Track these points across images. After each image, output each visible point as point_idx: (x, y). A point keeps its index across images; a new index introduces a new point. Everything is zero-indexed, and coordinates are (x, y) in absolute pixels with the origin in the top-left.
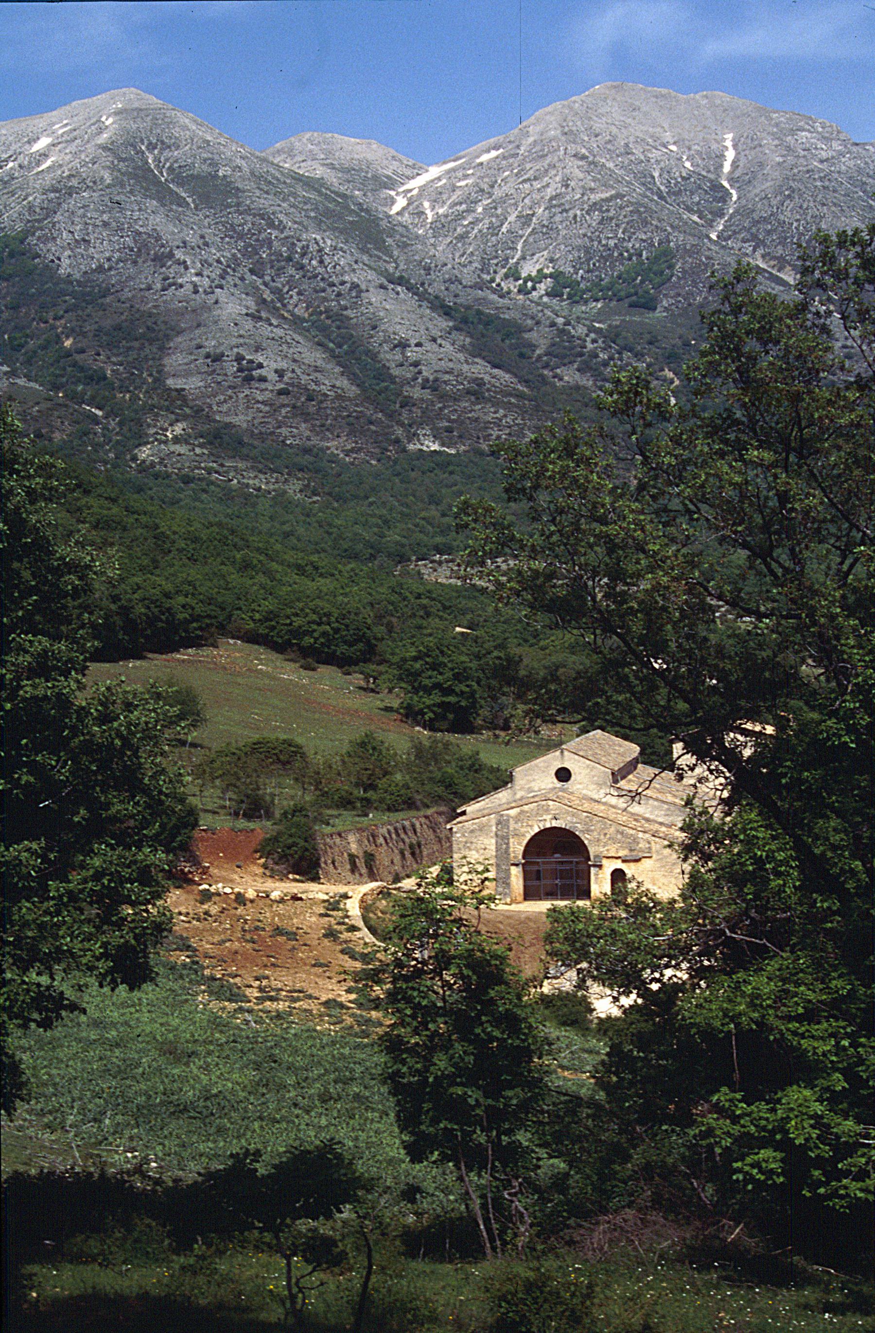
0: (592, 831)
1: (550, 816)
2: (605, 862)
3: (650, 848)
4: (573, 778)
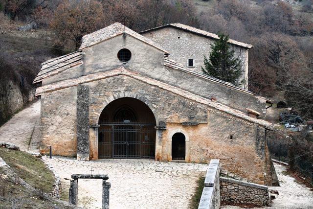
1: (123, 89)
2: (168, 128)
3: (206, 117)
4: (133, 57)
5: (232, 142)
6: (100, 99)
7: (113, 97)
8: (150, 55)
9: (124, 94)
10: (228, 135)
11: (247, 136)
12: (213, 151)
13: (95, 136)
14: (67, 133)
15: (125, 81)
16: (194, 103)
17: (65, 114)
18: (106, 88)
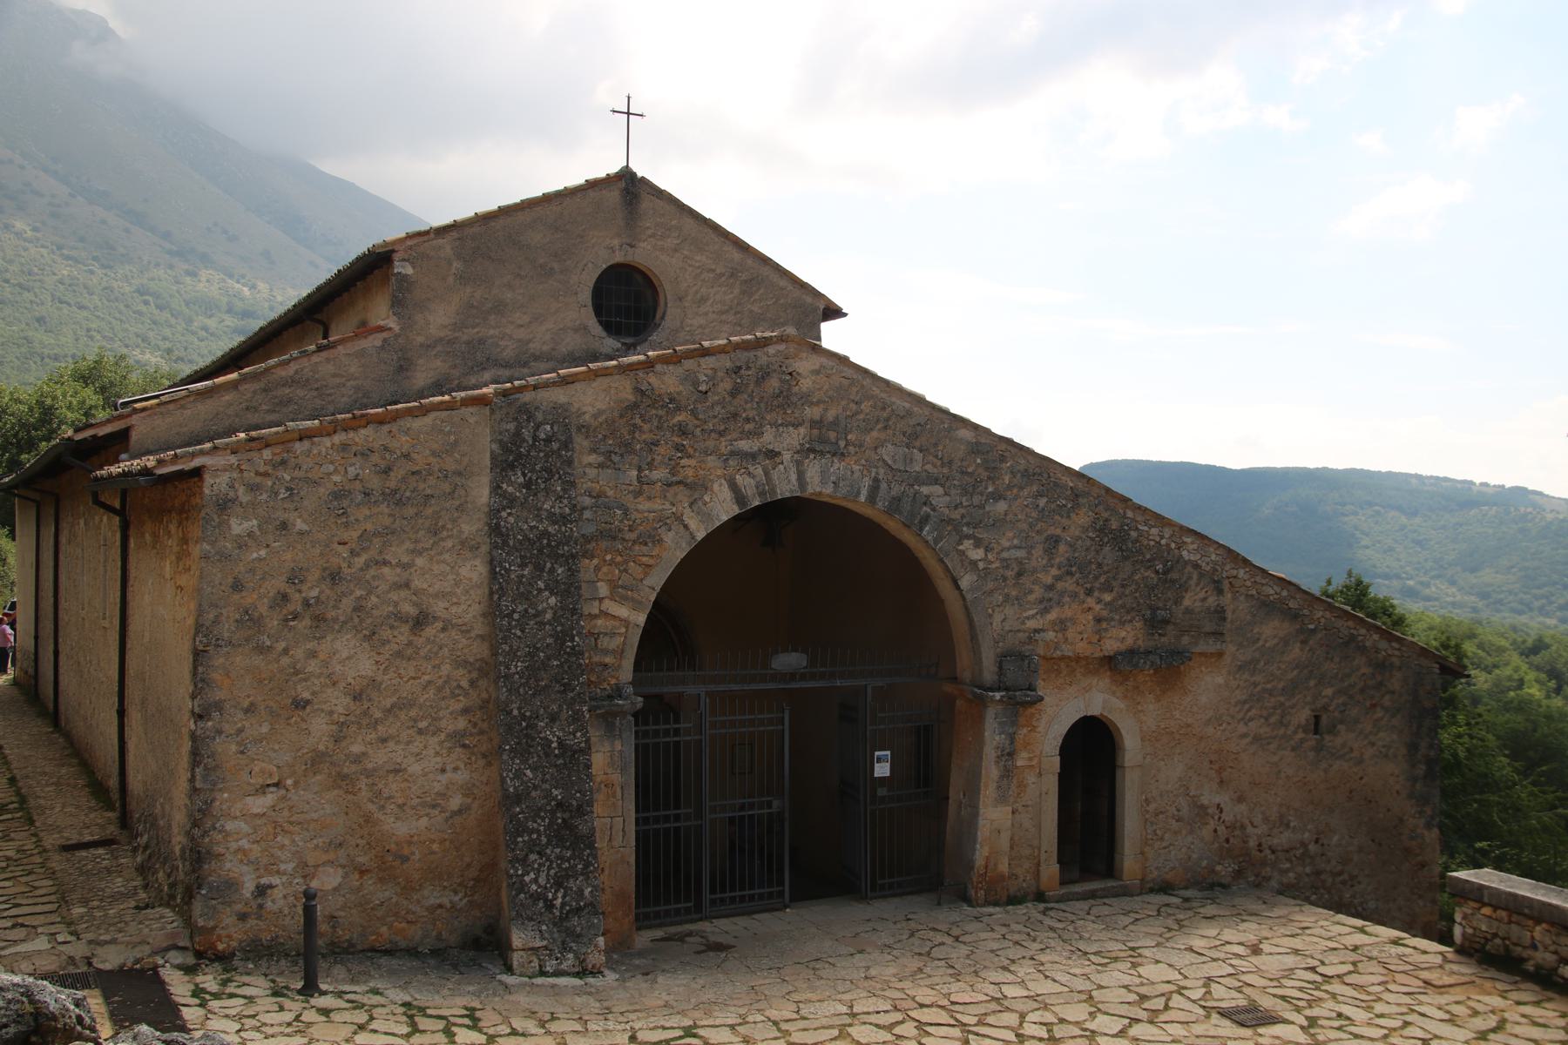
0: (999, 523)
1: (795, 437)
3: (1220, 613)
6: (645, 505)
8: (756, 309)
10: (1304, 715)
11: (1379, 713)
12: (1243, 807)
13: (616, 778)
14: (415, 768)
15: (806, 384)
16: (1167, 532)
17: (400, 618)
18: (683, 431)
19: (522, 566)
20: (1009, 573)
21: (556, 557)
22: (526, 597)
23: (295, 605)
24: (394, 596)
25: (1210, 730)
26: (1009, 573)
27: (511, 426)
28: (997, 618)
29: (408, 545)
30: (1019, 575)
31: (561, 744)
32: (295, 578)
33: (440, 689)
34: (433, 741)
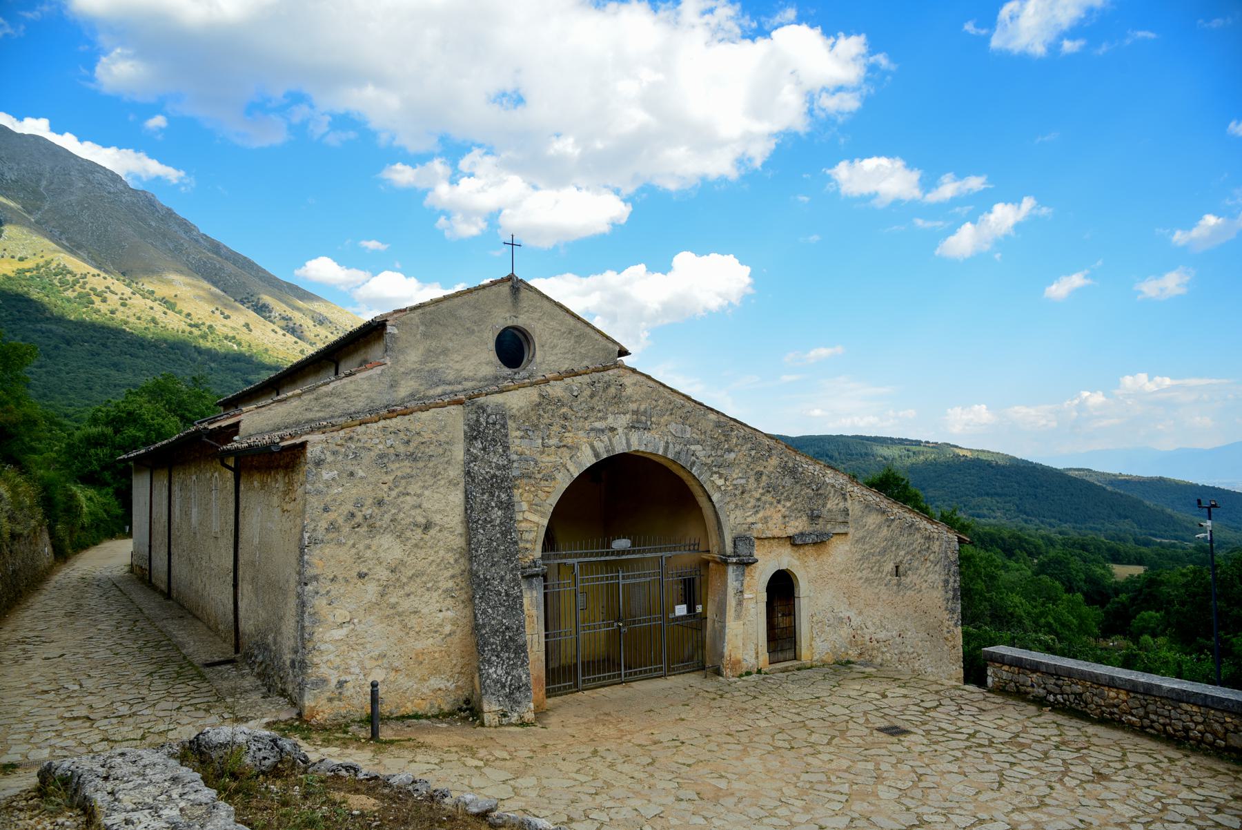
1: (624, 420)
5: (899, 585)
6: (546, 459)
7: (589, 452)
9: (628, 441)
10: (890, 566)
11: (929, 564)
14: (425, 611)
15: (629, 391)
19: (483, 494)
20: (737, 492)
21: (500, 489)
22: (485, 511)
23: (359, 519)
24: (413, 513)
25: (843, 576)
26: (737, 492)
27: (474, 417)
28: (732, 517)
29: (420, 483)
30: (743, 493)
31: (507, 595)
32: (359, 504)
33: (438, 565)
34: (435, 594)
